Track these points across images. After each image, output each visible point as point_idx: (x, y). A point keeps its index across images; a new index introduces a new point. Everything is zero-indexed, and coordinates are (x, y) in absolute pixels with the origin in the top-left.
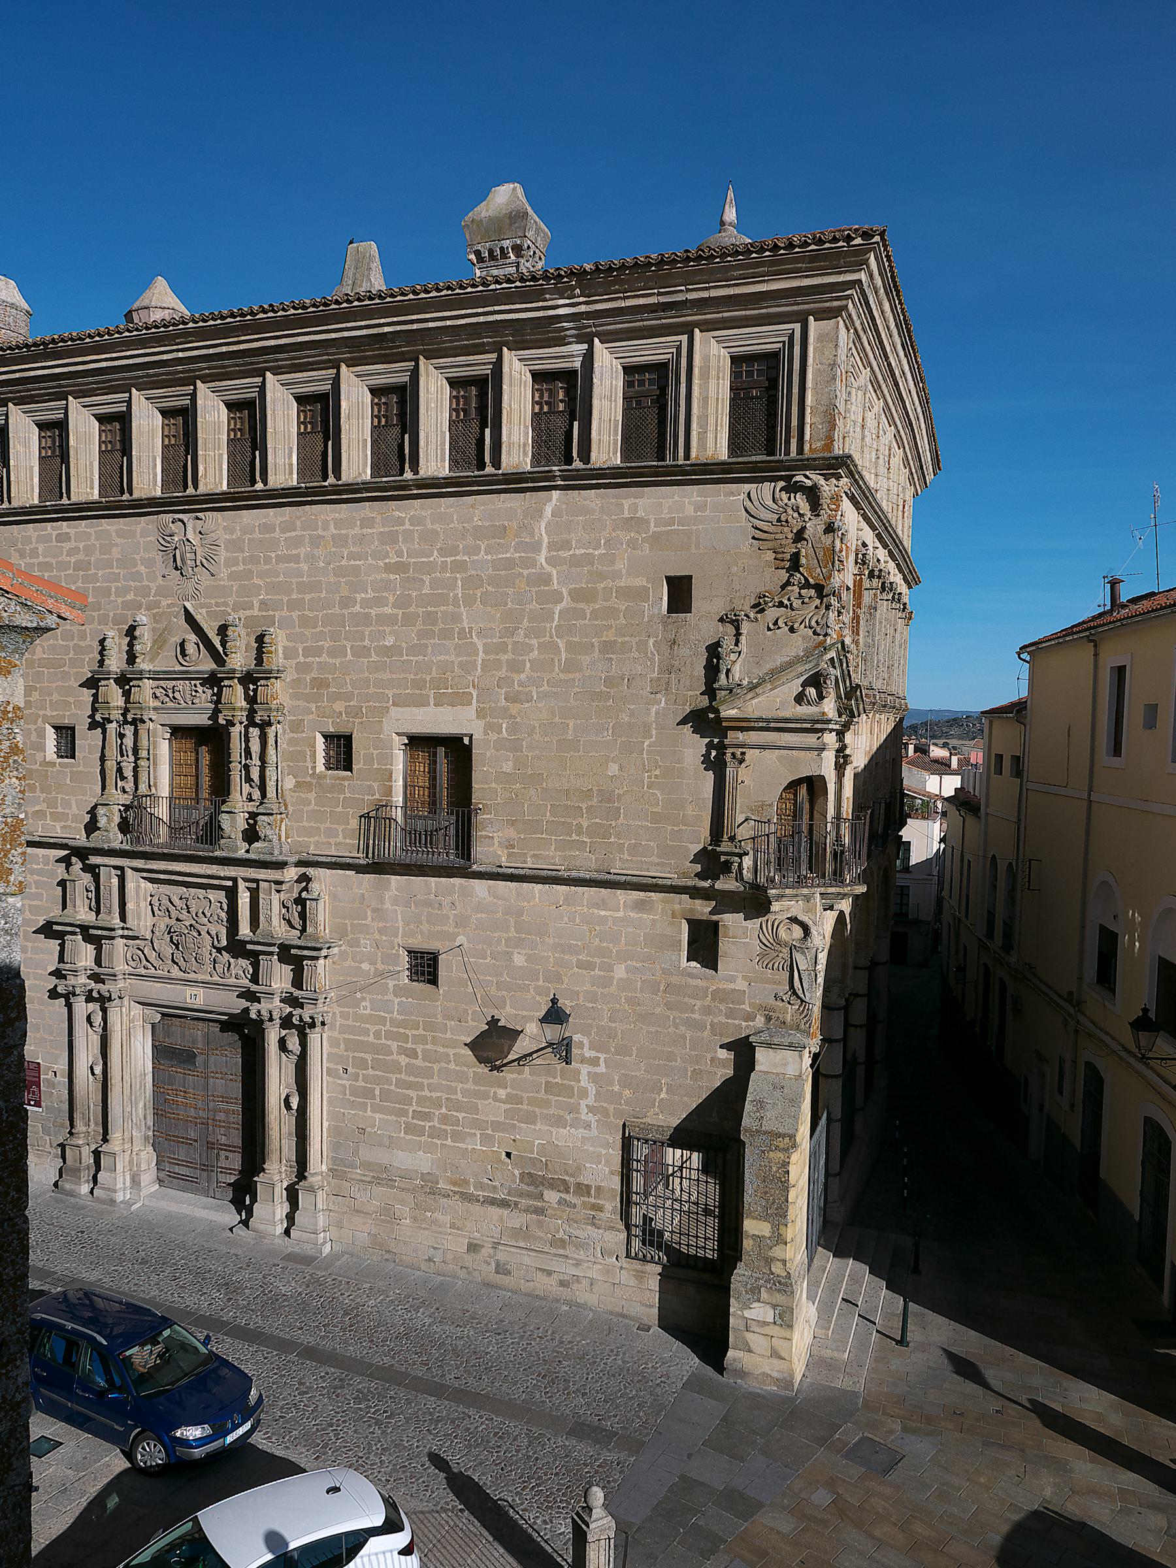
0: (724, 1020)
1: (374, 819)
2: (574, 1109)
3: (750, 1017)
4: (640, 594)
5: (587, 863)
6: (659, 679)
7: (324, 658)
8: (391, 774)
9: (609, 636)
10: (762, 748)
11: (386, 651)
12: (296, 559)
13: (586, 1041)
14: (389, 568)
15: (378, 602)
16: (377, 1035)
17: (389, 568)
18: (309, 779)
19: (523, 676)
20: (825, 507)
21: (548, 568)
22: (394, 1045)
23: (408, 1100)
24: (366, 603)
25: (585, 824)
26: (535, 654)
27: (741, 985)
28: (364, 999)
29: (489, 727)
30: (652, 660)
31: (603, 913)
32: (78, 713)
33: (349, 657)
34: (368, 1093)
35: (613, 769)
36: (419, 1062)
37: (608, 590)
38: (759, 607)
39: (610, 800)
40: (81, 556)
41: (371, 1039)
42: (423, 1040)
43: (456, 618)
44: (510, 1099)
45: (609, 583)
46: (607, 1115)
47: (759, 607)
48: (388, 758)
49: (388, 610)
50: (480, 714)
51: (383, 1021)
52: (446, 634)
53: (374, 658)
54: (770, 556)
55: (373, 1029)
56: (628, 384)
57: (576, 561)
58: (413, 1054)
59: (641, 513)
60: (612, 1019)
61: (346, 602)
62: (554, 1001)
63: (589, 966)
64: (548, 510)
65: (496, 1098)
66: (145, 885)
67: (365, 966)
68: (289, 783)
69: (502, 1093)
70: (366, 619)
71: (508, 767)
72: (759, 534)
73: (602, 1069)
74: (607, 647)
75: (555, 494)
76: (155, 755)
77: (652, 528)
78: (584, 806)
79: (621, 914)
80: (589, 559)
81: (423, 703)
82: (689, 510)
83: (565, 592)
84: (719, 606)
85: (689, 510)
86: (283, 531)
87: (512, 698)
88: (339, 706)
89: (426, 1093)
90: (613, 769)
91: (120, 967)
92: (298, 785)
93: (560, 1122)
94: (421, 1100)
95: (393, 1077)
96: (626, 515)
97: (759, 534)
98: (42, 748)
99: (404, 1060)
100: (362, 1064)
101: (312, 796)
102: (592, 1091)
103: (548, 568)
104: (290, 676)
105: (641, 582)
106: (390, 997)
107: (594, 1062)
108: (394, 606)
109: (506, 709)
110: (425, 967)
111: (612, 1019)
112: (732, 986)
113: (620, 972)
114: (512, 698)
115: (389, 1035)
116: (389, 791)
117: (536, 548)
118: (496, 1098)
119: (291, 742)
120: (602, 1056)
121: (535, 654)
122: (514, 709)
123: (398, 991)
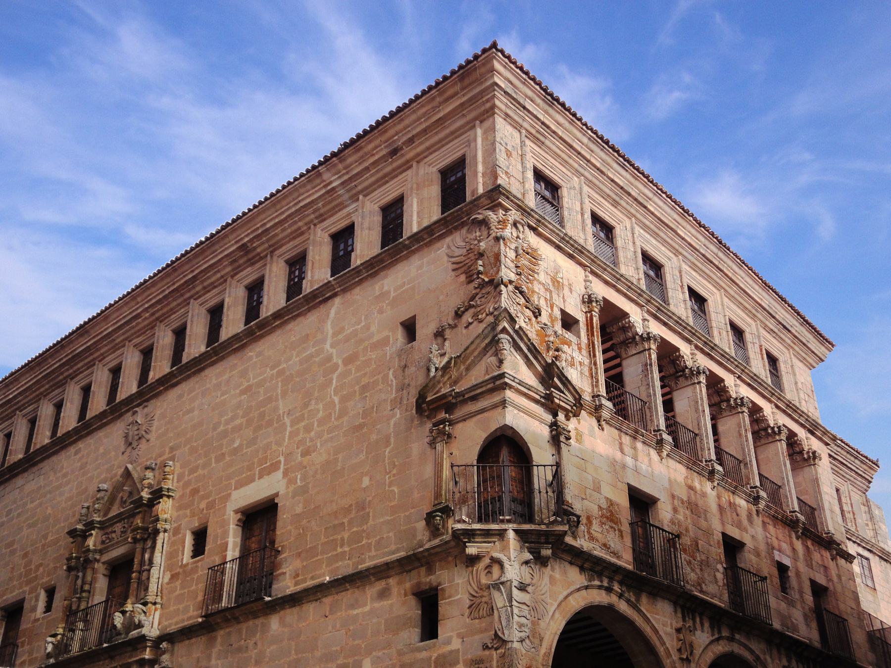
1: (215, 589)
4: (385, 342)
6: (395, 398)
7: (200, 472)
9: (365, 381)
10: (464, 419)
11: (235, 451)
12: (191, 410)
14: (243, 392)
15: (233, 419)
17: (243, 392)
18: (178, 570)
19: (313, 434)
20: (493, 227)
24: (227, 422)
25: (346, 536)
26: (321, 414)
27: (456, 644)
29: (291, 481)
30: (391, 386)
31: (356, 612)
32: (59, 576)
33: (214, 465)
35: (366, 482)
37: (365, 349)
38: (458, 315)
40: (84, 460)
43: (276, 409)
45: (367, 343)
47: (458, 315)
48: (226, 534)
49: (238, 422)
50: (285, 474)
52: (270, 423)
54: (463, 278)
56: (384, 218)
57: (347, 340)
59: (386, 288)
70: (225, 434)
71: (299, 510)
72: (455, 266)
75: (337, 300)
76: (95, 588)
77: (393, 294)
78: (346, 521)
80: (355, 333)
81: (251, 480)
83: (340, 362)
84: (432, 328)
90: (366, 482)
96: (377, 293)
97: (455, 266)
98: (34, 609)
101: (178, 583)
103: (331, 350)
105: (386, 333)
108: (243, 417)
109: (301, 463)
114: (306, 453)
117: (324, 341)
119: (172, 544)
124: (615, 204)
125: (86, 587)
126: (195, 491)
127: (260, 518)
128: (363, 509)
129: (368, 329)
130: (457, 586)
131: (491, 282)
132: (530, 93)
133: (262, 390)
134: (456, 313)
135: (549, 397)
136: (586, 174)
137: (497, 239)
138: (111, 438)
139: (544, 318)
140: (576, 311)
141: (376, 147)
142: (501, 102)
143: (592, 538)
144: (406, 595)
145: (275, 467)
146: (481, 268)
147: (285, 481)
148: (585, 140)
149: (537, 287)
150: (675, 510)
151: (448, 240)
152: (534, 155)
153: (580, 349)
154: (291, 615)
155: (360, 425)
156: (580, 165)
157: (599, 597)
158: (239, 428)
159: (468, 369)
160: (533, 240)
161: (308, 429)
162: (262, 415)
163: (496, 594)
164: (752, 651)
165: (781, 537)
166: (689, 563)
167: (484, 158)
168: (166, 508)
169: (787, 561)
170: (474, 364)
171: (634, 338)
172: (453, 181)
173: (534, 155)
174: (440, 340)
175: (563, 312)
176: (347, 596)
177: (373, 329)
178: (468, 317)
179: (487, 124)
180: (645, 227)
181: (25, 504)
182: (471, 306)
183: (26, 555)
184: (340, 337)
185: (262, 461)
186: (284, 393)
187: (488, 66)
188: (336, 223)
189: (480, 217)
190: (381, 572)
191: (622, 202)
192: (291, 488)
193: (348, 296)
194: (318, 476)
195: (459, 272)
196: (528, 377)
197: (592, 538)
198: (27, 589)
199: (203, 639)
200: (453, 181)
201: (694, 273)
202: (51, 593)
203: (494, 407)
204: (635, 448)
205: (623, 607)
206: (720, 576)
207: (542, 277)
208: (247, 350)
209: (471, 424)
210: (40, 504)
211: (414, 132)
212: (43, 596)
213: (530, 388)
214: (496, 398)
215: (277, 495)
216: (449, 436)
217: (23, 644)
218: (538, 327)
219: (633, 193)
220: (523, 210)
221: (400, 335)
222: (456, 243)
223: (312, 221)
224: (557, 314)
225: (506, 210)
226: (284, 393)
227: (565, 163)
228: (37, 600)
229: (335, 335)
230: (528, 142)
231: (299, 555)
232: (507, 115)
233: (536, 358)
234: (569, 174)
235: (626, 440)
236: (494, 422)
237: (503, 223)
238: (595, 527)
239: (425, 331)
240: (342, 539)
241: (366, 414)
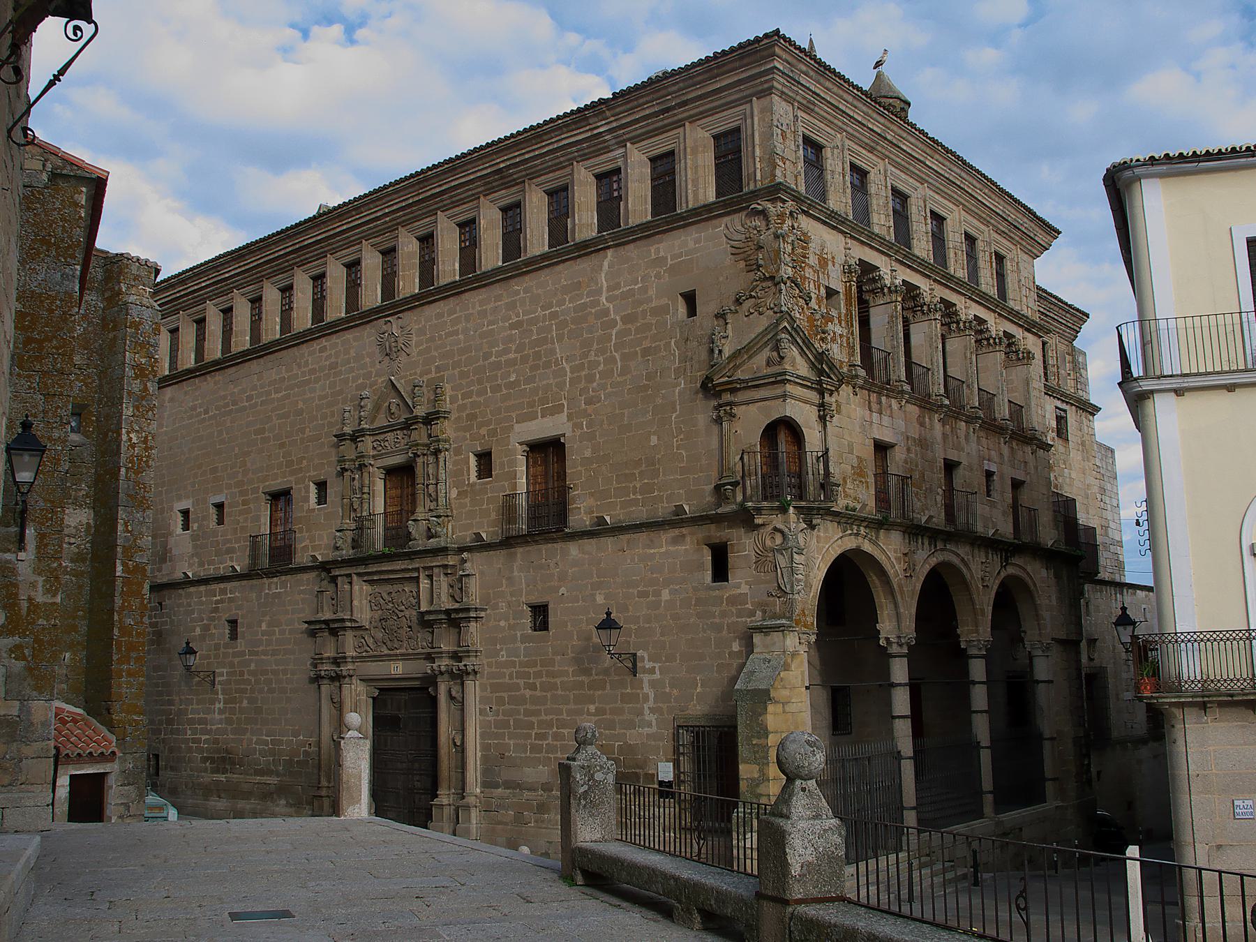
0: (734, 619)
1: (508, 509)
2: (640, 713)
3: (752, 614)
4: (663, 310)
5: (641, 513)
7: (474, 398)
8: (519, 476)
9: (646, 344)
10: (747, 403)
11: (511, 385)
12: (456, 333)
13: (646, 656)
14: (512, 327)
15: (506, 351)
16: (511, 677)
17: (512, 327)
21: (607, 305)
22: (521, 682)
23: (530, 726)
24: (499, 354)
26: (601, 367)
27: (744, 589)
28: (501, 649)
29: (577, 426)
30: (674, 355)
32: (328, 472)
34: (505, 724)
35: (654, 440)
36: (538, 693)
38: (738, 302)
39: (654, 464)
40: (333, 360)
41: (507, 680)
42: (538, 675)
43: (553, 352)
44: (599, 712)
45: (645, 306)
46: (662, 714)
47: (738, 302)
48: (513, 463)
49: (512, 356)
50: (570, 418)
51: (513, 664)
52: (547, 365)
53: (505, 391)
54: (742, 264)
55: (507, 671)
56: (653, 169)
57: (624, 296)
58: (533, 687)
59: (662, 254)
60: (662, 635)
61: (487, 356)
62: (609, 614)
63: (643, 595)
64: (606, 264)
65: (589, 714)
66: (366, 587)
67: (502, 623)
68: (454, 493)
69: (592, 708)
70: (497, 366)
71: (588, 453)
72: (735, 251)
73: (657, 676)
74: (646, 352)
75: (610, 253)
77: (669, 262)
78: (636, 472)
79: (663, 550)
80: (631, 293)
82: (691, 244)
84: (713, 308)
85: (691, 244)
86: (449, 315)
87: (589, 402)
88: (483, 431)
89: (543, 717)
90: (654, 440)
91: (351, 653)
92: (459, 494)
93: (632, 725)
94: (541, 723)
95: (522, 709)
96: (653, 256)
97: (735, 251)
98: (307, 499)
99: (528, 693)
100: (500, 701)
101: (468, 500)
102: (652, 696)
103: (607, 305)
104: (453, 416)
105: (664, 301)
106: (519, 644)
107: (652, 671)
109: (585, 410)
110: (540, 613)
111: (662, 635)
112: (739, 591)
113: (665, 595)
114: (589, 402)
115: (520, 675)
116: (514, 486)
117: (599, 292)
118: (589, 714)
119: (455, 463)
120: (657, 665)
121: (601, 367)
122: (590, 409)
123: (525, 639)
124: (871, 150)
125: (366, 490)
126: (472, 417)
127: (548, 452)
128: (654, 464)
129: (646, 292)
130: (744, 546)
131: (772, 278)
132: (804, 68)
133: (534, 328)
134: (737, 300)
135: (820, 383)
136: (848, 129)
137: (777, 237)
138: (364, 340)
139: (813, 304)
140: (837, 284)
141: (648, 102)
142: (779, 82)
143: (846, 496)
144: (698, 544)
145: (558, 409)
146: (761, 262)
147: (570, 424)
148: (850, 99)
149: (809, 273)
150: (908, 450)
151: (726, 219)
152: (807, 124)
153: (840, 322)
154: (590, 544)
155: (644, 385)
156: (843, 123)
157: (850, 543)
158: (512, 363)
159: (750, 358)
160: (805, 223)
161: (590, 379)
162: (537, 355)
163: (779, 557)
164: (958, 555)
165: (991, 446)
166: (917, 494)
167: (762, 141)
168: (447, 429)
169: (993, 468)
170: (755, 353)
171: (882, 289)
172: (729, 150)
173: (807, 124)
174: (721, 322)
175: (827, 288)
176: (643, 537)
177: (652, 292)
178: (748, 304)
179: (765, 101)
180: (897, 165)
181: (268, 393)
182: (751, 297)
183: (282, 445)
184: (617, 292)
185: (543, 401)
186: (560, 338)
187: (771, 51)
188: (603, 163)
189: (760, 208)
190: (677, 520)
191: (879, 148)
192: (578, 433)
193: (621, 250)
194: (605, 426)
195: (738, 257)
196: (803, 368)
197: (846, 496)
198: (292, 478)
199: (503, 552)
200: (729, 150)
201: (937, 197)
202: (322, 486)
203: (777, 398)
204: (880, 403)
205: (867, 547)
206: (939, 498)
207: (813, 260)
208: (513, 282)
209: (753, 408)
210: (287, 397)
211: (690, 96)
212: (313, 489)
213: (804, 379)
214: (778, 391)
215: (564, 435)
216: (733, 416)
217: (301, 530)
218: (808, 313)
219: (889, 137)
220: (797, 198)
221: (682, 309)
222: (735, 224)
223: (574, 158)
224: (823, 291)
225: (784, 202)
226: (560, 338)
227: (830, 124)
228: (307, 491)
229: (609, 289)
230: (800, 113)
231: (592, 495)
232: (783, 93)
233: (808, 348)
234: (833, 132)
235: (874, 397)
236: (778, 410)
237: (781, 216)
238: (849, 485)
239: (706, 308)
240: (635, 487)
241: (649, 377)
